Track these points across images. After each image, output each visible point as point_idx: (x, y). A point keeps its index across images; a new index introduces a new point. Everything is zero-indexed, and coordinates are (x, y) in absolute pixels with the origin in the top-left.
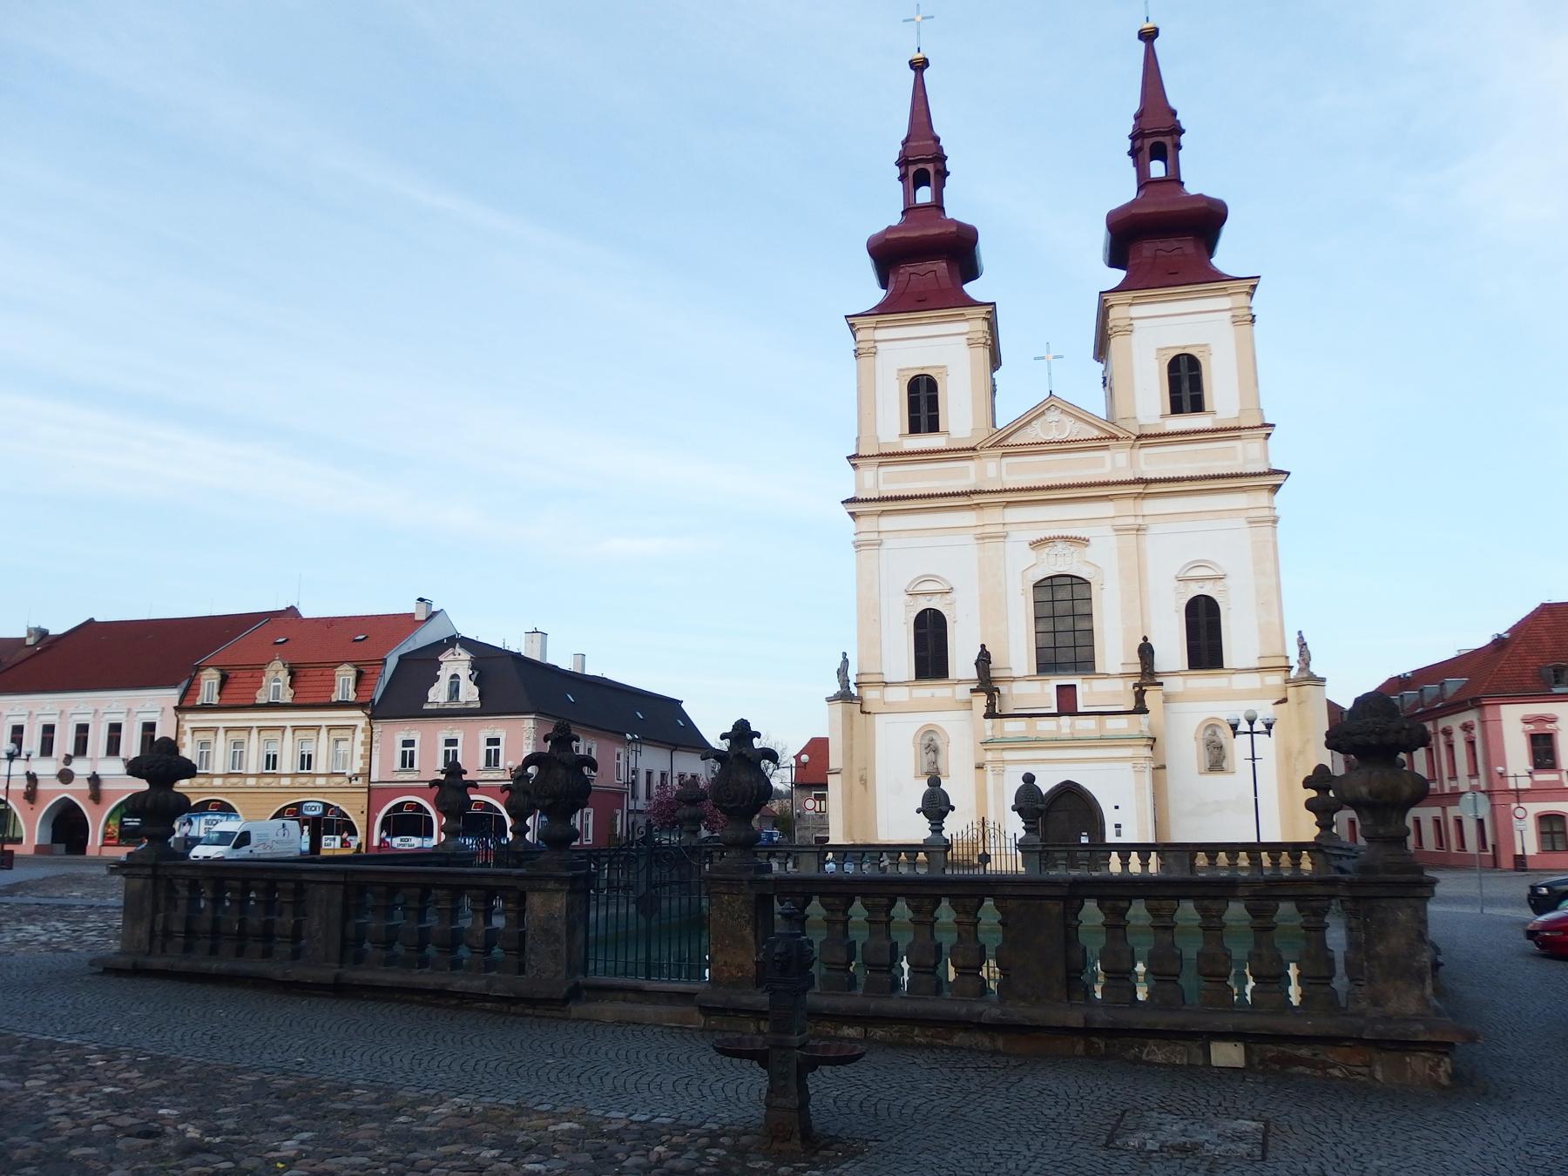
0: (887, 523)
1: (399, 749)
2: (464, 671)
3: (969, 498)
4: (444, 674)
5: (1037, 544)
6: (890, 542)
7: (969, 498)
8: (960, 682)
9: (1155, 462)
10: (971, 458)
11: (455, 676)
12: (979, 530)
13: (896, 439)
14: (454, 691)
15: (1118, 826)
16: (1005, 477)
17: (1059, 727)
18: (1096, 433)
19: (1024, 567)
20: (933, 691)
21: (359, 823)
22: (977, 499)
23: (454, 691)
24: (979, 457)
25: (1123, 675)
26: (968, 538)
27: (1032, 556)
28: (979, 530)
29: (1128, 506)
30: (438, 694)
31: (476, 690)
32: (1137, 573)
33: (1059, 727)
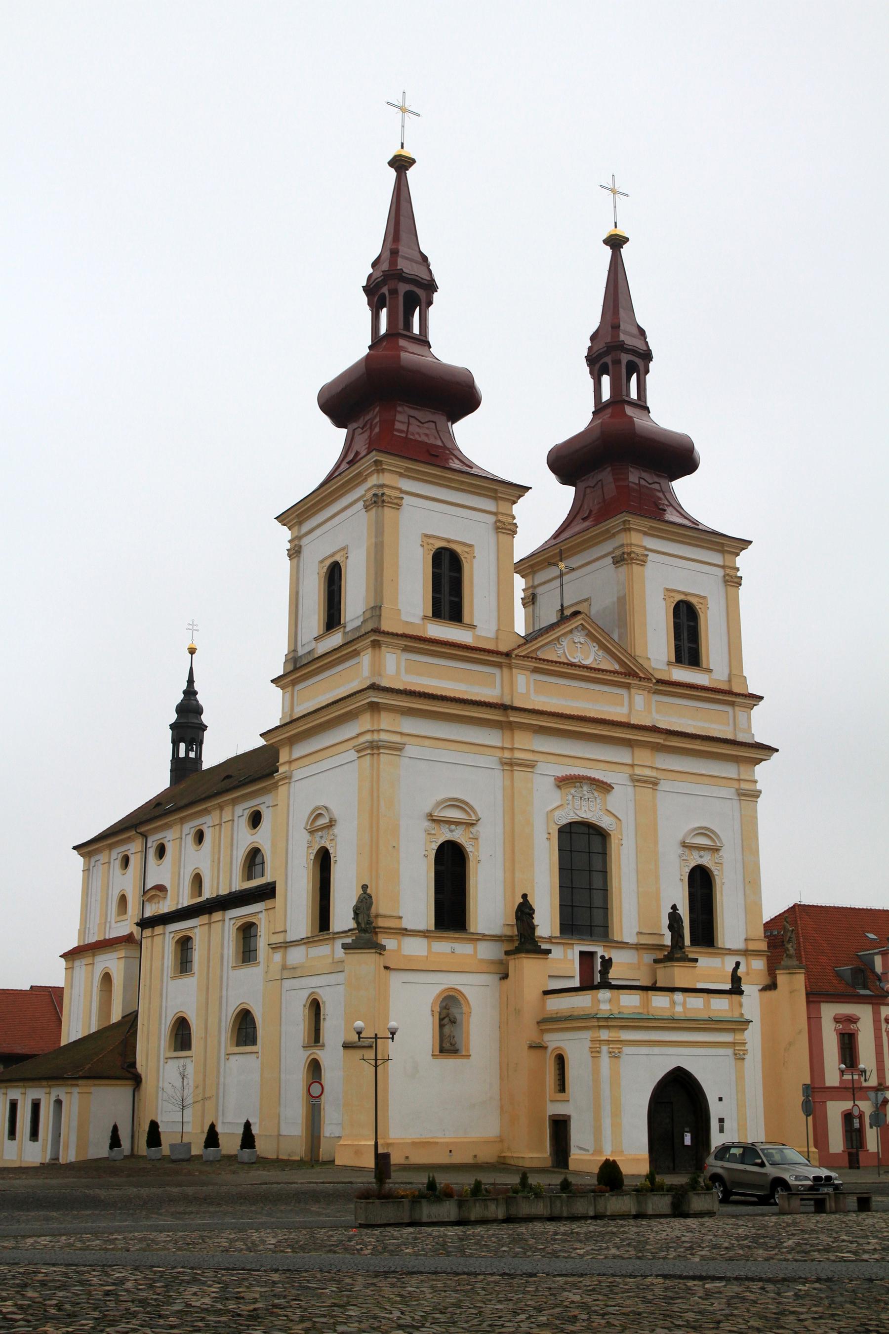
0: (409, 725)
3: (503, 715)
5: (564, 782)
6: (411, 750)
7: (503, 715)
8: (484, 937)
9: (640, 707)
10: (499, 665)
12: (507, 754)
13: (417, 621)
15: (721, 1120)
16: (533, 696)
17: (673, 1003)
18: (617, 667)
19: (548, 809)
20: (447, 947)
22: (514, 718)
24: (510, 667)
26: (490, 761)
27: (555, 798)
28: (507, 754)
29: (643, 756)
32: (648, 833)
33: (673, 1003)
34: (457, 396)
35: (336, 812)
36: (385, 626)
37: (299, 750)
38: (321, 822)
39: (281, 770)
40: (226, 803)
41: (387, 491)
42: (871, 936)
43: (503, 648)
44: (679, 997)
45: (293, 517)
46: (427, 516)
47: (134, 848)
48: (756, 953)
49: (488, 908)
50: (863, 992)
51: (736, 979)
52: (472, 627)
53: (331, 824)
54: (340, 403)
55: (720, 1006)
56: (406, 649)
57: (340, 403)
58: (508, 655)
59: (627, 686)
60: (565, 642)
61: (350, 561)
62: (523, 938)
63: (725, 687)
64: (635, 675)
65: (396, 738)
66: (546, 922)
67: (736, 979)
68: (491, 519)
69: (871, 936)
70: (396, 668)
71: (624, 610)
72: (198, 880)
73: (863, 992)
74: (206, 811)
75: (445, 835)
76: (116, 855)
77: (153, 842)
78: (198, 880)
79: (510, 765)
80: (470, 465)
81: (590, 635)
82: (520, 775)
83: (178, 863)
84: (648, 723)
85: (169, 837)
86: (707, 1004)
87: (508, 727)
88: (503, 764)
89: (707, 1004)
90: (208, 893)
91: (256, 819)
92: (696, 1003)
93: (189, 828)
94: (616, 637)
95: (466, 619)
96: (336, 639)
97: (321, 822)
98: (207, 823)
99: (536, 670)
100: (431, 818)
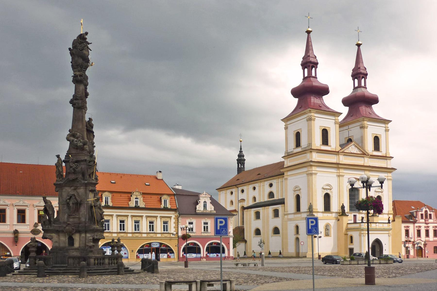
0: (318, 169)
1: (203, 225)
2: (208, 201)
3: (337, 166)
4: (202, 201)
6: (318, 174)
7: (337, 166)
10: (336, 154)
11: (205, 202)
13: (319, 146)
14: (205, 206)
21: (175, 250)
23: (205, 206)
25: (336, 213)
30: (200, 208)
31: (213, 208)
34: (323, 91)
35: (301, 187)
36: (313, 148)
37: (289, 173)
38: (297, 189)
39: (285, 177)
40: (263, 181)
41: (312, 117)
42: (413, 207)
43: (337, 151)
44: (377, 224)
45: (286, 120)
46: (321, 122)
47: (234, 190)
48: (391, 214)
49: (335, 207)
50: (411, 220)
51: (389, 220)
52: (330, 146)
53: (300, 190)
54: (296, 93)
55: (386, 226)
56: (317, 152)
57: (296, 93)
58: (338, 152)
59: (363, 157)
60: (350, 148)
61: (302, 132)
62: (343, 213)
63: (385, 155)
64: (365, 154)
65: (316, 172)
66: (347, 209)
67: (389, 220)
68: (334, 121)
69: (413, 207)
70: (315, 157)
71: (362, 139)
72: (255, 198)
73: (411, 220)
74: (256, 183)
75: (326, 192)
76: (229, 191)
77: (240, 189)
78: (255, 198)
79: (339, 176)
80: (328, 108)
81: (356, 146)
82: (341, 178)
83: (248, 194)
84: (368, 165)
85: (245, 188)
86: (383, 226)
87: (338, 168)
88: (337, 176)
89: (383, 226)
90: (257, 201)
91: (271, 185)
92: (381, 225)
93: (251, 187)
94: (360, 145)
95: (329, 145)
96: (299, 149)
97: (297, 189)
98: (257, 185)
99: (344, 155)
100: (323, 188)
